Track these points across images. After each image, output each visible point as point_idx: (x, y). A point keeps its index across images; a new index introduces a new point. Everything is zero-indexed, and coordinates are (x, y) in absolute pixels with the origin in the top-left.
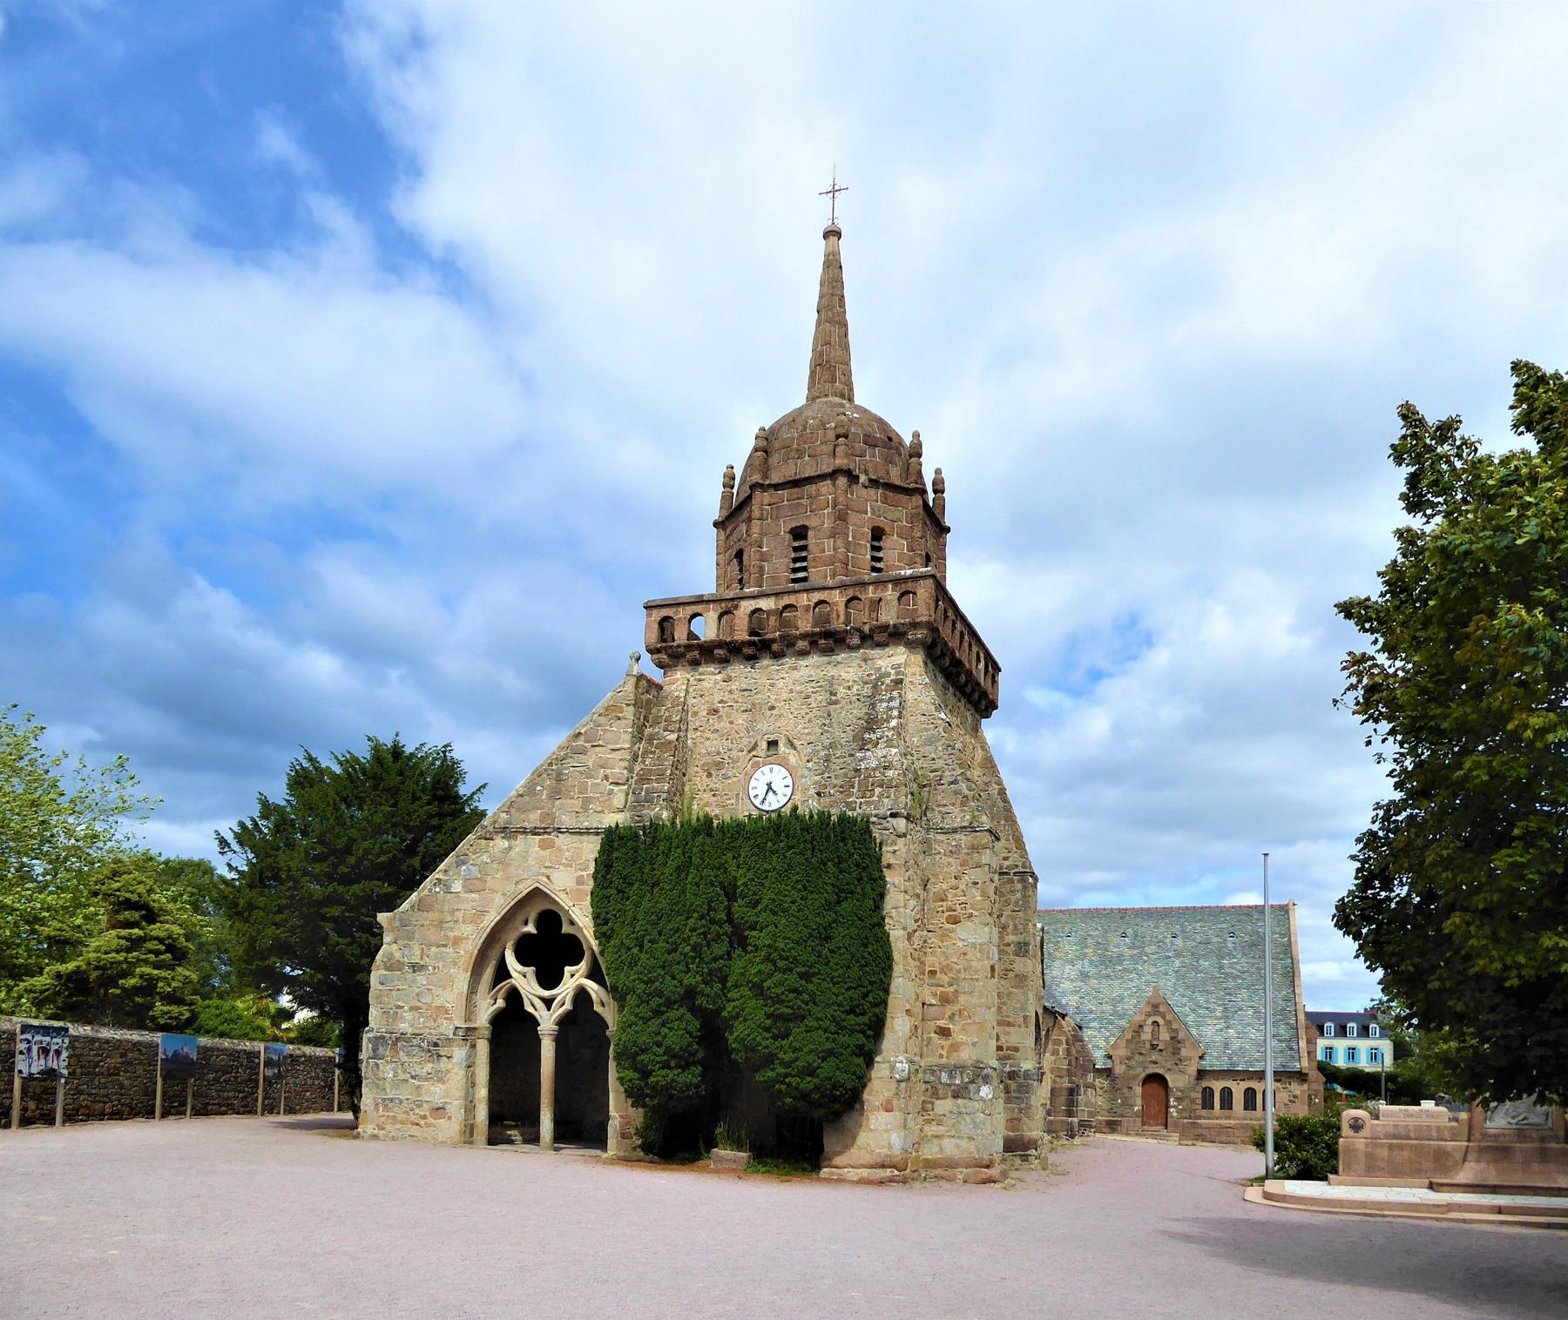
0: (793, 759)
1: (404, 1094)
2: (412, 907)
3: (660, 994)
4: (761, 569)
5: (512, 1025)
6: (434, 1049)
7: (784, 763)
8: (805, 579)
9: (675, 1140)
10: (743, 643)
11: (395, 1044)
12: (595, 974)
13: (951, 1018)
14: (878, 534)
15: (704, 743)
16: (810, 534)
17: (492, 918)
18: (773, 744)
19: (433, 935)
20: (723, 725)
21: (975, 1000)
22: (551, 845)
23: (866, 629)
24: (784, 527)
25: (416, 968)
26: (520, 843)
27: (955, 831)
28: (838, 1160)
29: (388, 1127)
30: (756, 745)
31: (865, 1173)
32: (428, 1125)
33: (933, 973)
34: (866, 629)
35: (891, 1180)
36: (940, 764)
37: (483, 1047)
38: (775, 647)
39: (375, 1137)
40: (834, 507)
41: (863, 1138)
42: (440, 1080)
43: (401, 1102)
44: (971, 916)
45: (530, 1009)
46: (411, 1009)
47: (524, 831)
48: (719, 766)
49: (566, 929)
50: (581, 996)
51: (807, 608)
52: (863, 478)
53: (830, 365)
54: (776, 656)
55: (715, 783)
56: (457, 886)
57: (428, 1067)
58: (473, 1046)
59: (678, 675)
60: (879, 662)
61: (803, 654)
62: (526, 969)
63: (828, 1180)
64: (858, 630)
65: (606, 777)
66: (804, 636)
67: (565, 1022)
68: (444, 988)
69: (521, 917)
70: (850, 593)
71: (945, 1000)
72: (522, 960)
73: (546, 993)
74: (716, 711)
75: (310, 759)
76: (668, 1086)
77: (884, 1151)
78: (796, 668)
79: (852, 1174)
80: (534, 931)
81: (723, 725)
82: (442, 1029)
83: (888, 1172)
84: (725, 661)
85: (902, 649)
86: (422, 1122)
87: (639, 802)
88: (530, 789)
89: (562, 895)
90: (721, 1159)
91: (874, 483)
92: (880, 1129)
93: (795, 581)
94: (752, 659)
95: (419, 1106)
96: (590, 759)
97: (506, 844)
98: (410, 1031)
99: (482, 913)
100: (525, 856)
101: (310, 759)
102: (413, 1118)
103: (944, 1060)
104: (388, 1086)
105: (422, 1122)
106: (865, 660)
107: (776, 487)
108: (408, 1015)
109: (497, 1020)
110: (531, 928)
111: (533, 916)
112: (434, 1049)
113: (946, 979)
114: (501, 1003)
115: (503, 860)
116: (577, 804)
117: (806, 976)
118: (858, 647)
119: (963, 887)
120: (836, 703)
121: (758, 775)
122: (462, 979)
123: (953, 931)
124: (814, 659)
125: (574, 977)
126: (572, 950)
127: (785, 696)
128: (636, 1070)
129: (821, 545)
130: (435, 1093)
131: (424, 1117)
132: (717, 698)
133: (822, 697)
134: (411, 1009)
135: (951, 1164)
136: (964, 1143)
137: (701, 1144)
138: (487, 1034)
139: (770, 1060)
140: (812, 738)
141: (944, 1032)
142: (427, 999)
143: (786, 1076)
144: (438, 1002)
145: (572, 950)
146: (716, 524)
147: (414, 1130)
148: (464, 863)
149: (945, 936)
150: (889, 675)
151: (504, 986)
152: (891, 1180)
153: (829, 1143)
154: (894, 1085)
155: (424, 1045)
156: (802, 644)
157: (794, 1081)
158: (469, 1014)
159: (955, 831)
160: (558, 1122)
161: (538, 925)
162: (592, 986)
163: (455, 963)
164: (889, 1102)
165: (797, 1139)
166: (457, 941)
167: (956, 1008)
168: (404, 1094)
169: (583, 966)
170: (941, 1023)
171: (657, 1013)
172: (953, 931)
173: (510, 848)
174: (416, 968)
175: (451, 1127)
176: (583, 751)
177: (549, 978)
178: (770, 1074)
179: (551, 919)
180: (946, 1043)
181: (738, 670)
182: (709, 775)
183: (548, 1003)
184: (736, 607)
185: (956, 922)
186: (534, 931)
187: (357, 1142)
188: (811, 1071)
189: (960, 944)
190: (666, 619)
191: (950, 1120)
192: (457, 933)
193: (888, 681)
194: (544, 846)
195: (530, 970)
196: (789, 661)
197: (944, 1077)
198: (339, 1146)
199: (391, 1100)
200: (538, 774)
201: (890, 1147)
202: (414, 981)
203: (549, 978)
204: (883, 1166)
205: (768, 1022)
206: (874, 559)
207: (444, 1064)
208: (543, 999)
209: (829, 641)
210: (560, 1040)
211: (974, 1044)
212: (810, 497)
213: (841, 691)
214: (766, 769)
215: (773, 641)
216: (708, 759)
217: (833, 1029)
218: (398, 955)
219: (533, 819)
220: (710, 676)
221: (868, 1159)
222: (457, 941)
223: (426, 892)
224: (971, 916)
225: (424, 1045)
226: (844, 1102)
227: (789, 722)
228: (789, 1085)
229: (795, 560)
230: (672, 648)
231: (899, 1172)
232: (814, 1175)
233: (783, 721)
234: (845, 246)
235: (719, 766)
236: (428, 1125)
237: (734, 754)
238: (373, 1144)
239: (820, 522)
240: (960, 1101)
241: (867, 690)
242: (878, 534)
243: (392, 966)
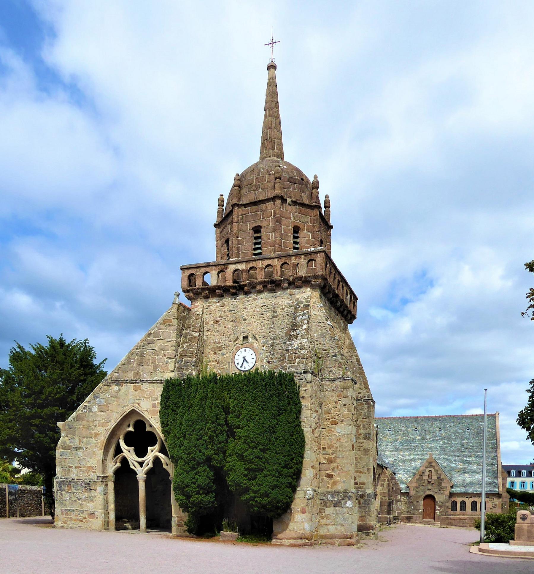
0: (256, 345)
1: (75, 507)
2: (74, 419)
3: (194, 460)
4: (238, 248)
5: (124, 476)
6: (88, 486)
7: (251, 347)
8: (260, 254)
9: (203, 527)
10: (230, 287)
11: (69, 484)
12: (163, 450)
13: (333, 469)
14: (296, 230)
15: (212, 338)
16: (263, 230)
17: (113, 424)
18: (246, 338)
19: (84, 433)
20: (221, 328)
21: (345, 461)
23: (291, 279)
24: (249, 226)
25: (77, 448)
26: (124, 387)
27: (335, 380)
28: (279, 536)
29: (69, 523)
30: (237, 338)
31: (292, 541)
32: (87, 522)
33: (324, 448)
34: (291, 279)
35: (305, 545)
36: (327, 347)
37: (111, 485)
38: (246, 289)
39: (62, 527)
40: (274, 216)
41: (291, 526)
42: (92, 501)
43: (74, 511)
44: (343, 421)
45: (132, 467)
46: (76, 468)
47: (126, 382)
48: (219, 348)
49: (148, 429)
50: (157, 461)
51: (261, 269)
52: (289, 200)
53: (272, 140)
54: (247, 293)
55: (218, 357)
56: (95, 409)
57: (86, 495)
58: (107, 485)
59: (198, 303)
60: (298, 296)
61: (260, 292)
62: (130, 448)
63: (275, 545)
64: (287, 280)
65: (165, 355)
66: (260, 283)
67: (149, 473)
68: (91, 458)
69: (126, 423)
70: (283, 260)
71: (330, 461)
72: (128, 444)
73: (140, 460)
74: (218, 321)
75: (20, 347)
76: (199, 503)
77: (302, 531)
78: (256, 299)
79: (287, 542)
80: (133, 430)
81: (221, 328)
82: (91, 477)
83: (303, 541)
84: (221, 296)
85: (309, 289)
86: (84, 520)
87: (181, 367)
88: (128, 361)
89: (146, 413)
90: (225, 536)
91: (294, 203)
92: (300, 521)
93: (255, 254)
94: (235, 295)
95: (83, 513)
96: (157, 346)
98: (76, 478)
99: (108, 422)
100: (127, 394)
101: (20, 347)
102: (80, 518)
103: (329, 489)
104: (67, 503)
105: (84, 520)
106: (291, 295)
107: (245, 205)
108: (75, 471)
109: (118, 473)
110: (131, 429)
111: (132, 423)
112: (88, 486)
114: (118, 465)
115: (116, 396)
116: (151, 368)
117: (264, 451)
118: (287, 288)
119: (339, 407)
120: (276, 317)
121: (239, 353)
122: (100, 454)
123: (334, 428)
124: (266, 295)
125: (153, 452)
126: (152, 439)
127: (251, 313)
128: (184, 495)
129: (268, 236)
130: (90, 506)
131: (85, 518)
132: (218, 315)
133: (270, 314)
134: (76, 468)
135: (333, 537)
136: (339, 528)
137: (215, 529)
138: (113, 479)
139: (247, 490)
140: (265, 334)
141: (330, 476)
142: (83, 463)
143: (255, 497)
144: (89, 464)
145: (152, 439)
146: (215, 225)
147: (81, 524)
148: (97, 398)
149: (330, 431)
150: (302, 302)
151: (120, 456)
152: (305, 545)
153: (276, 528)
154: (306, 501)
155: (83, 484)
156: (259, 287)
157: (259, 500)
158: (104, 470)
159: (335, 380)
160: (148, 519)
161: (135, 427)
162: (161, 456)
163: (96, 446)
164: (304, 509)
165: (261, 525)
166: (96, 435)
167: (335, 465)
168: (75, 507)
169: (157, 447)
170: (328, 472)
171: (193, 468)
172: (334, 428)
173: (120, 390)
174: (77, 448)
175: (98, 522)
176: (153, 342)
177: (141, 452)
178: (247, 496)
179: (141, 424)
180: (331, 481)
181: (228, 300)
182: (215, 353)
183: (141, 464)
185: (335, 424)
186: (133, 430)
187: (54, 529)
188: (267, 495)
189: (337, 434)
190: (192, 275)
191: (332, 517)
192: (96, 431)
193: (302, 305)
194: (136, 389)
195: (132, 449)
196: (253, 296)
197: (330, 497)
198: (46, 531)
199: (69, 510)
200: (131, 353)
201: (304, 530)
202: (77, 454)
203: (141, 452)
204: (301, 538)
205: (246, 472)
206: (295, 243)
207: (93, 493)
208: (138, 462)
209: (273, 285)
210: (147, 481)
211: (344, 482)
212: (262, 211)
213: (279, 311)
214: (243, 350)
215: (245, 285)
216: (214, 345)
217: (277, 475)
218: (68, 442)
219: (130, 376)
220: (214, 304)
221: (294, 535)
222: (96, 435)
223: (80, 412)
224: (343, 421)
225: (83, 484)
226: (283, 509)
227: (254, 327)
228: (256, 501)
229: (255, 244)
230: (195, 290)
231: (308, 541)
232: (269, 543)
233: (250, 327)
235: (219, 348)
236: (87, 522)
237: (227, 343)
238: (62, 530)
239: (267, 224)
240: (337, 508)
241: (292, 310)
242: (296, 230)
243: (66, 447)
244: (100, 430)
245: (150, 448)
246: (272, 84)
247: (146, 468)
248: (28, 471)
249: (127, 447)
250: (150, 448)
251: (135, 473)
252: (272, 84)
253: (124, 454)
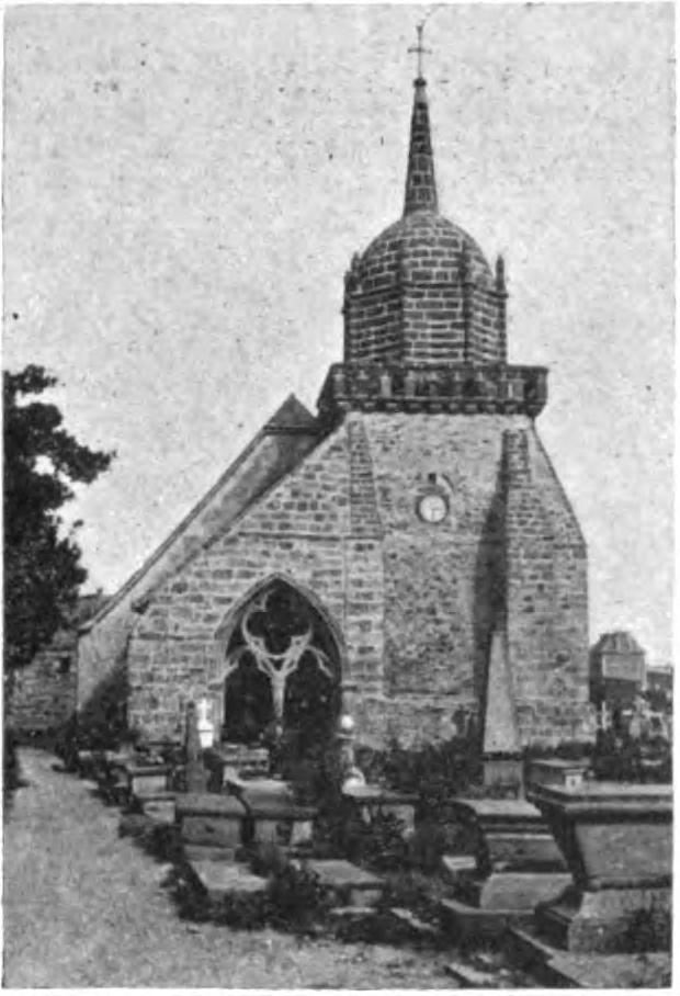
22: (289, 546)
45: (261, 667)
50: (307, 660)
73: (277, 657)
110: (263, 607)
114: (236, 665)
151: (239, 652)
161: (268, 604)
169: (308, 636)
203: (278, 644)
208: (272, 660)
234: (430, 91)
244: (214, 609)
245: (294, 639)
246: (421, 107)
248: (472, 803)
249: (254, 639)
250: (294, 639)
252: (421, 107)
253: (248, 648)
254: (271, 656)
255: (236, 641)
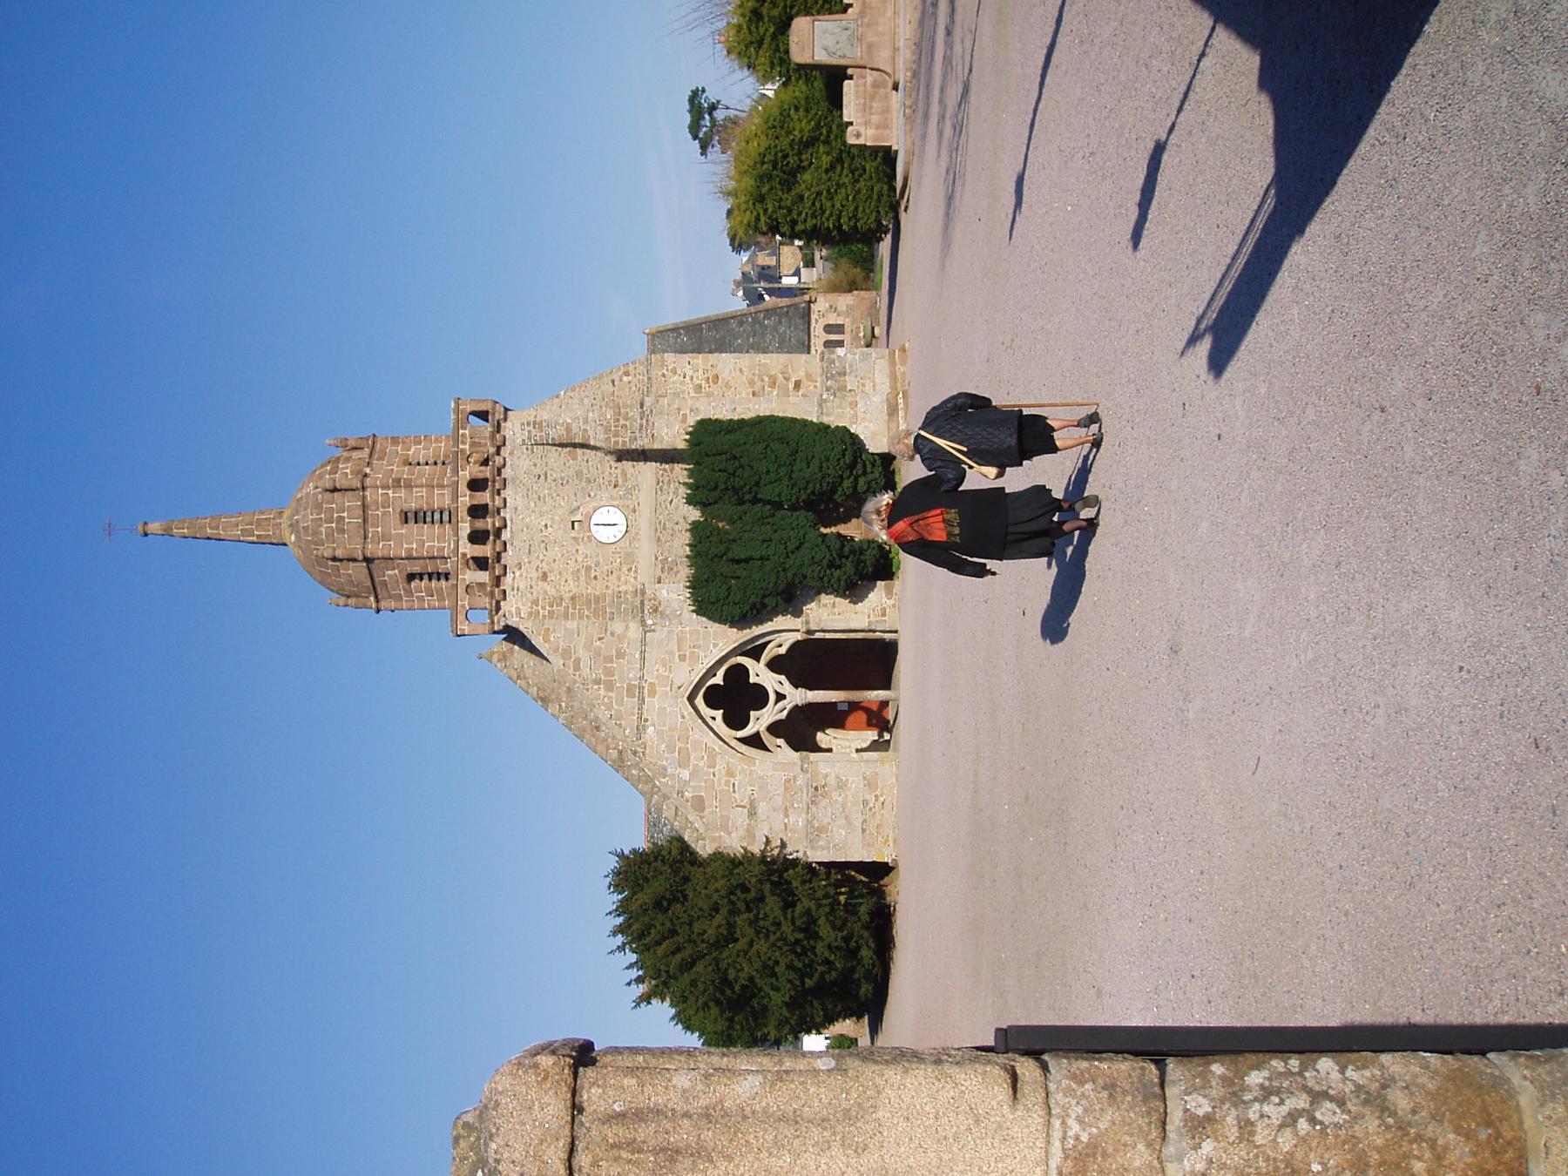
13: (787, 379)
16: (406, 507)
40: (388, 488)
49: (718, 679)
50: (775, 665)
60: (519, 441)
73: (772, 697)
97: (651, 728)
110: (719, 714)
113: (759, 383)
114: (780, 741)
125: (759, 673)
129: (415, 499)
141: (798, 385)
151: (767, 738)
162: (767, 655)
170: (791, 386)
174: (752, 814)
176: (578, 660)
177: (759, 697)
184: (464, 555)
194: (652, 693)
199: (864, 831)
203: (759, 697)
207: (832, 780)
208: (777, 702)
222: (730, 773)
247: (787, 688)
251: (796, 710)
254: (733, 732)
255: (755, 741)
